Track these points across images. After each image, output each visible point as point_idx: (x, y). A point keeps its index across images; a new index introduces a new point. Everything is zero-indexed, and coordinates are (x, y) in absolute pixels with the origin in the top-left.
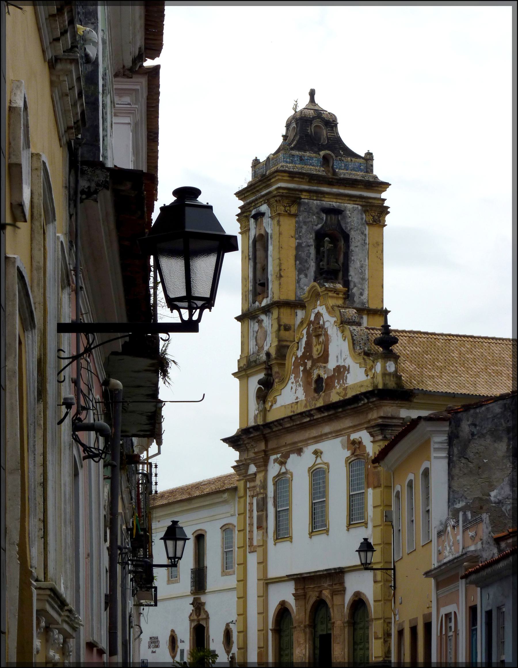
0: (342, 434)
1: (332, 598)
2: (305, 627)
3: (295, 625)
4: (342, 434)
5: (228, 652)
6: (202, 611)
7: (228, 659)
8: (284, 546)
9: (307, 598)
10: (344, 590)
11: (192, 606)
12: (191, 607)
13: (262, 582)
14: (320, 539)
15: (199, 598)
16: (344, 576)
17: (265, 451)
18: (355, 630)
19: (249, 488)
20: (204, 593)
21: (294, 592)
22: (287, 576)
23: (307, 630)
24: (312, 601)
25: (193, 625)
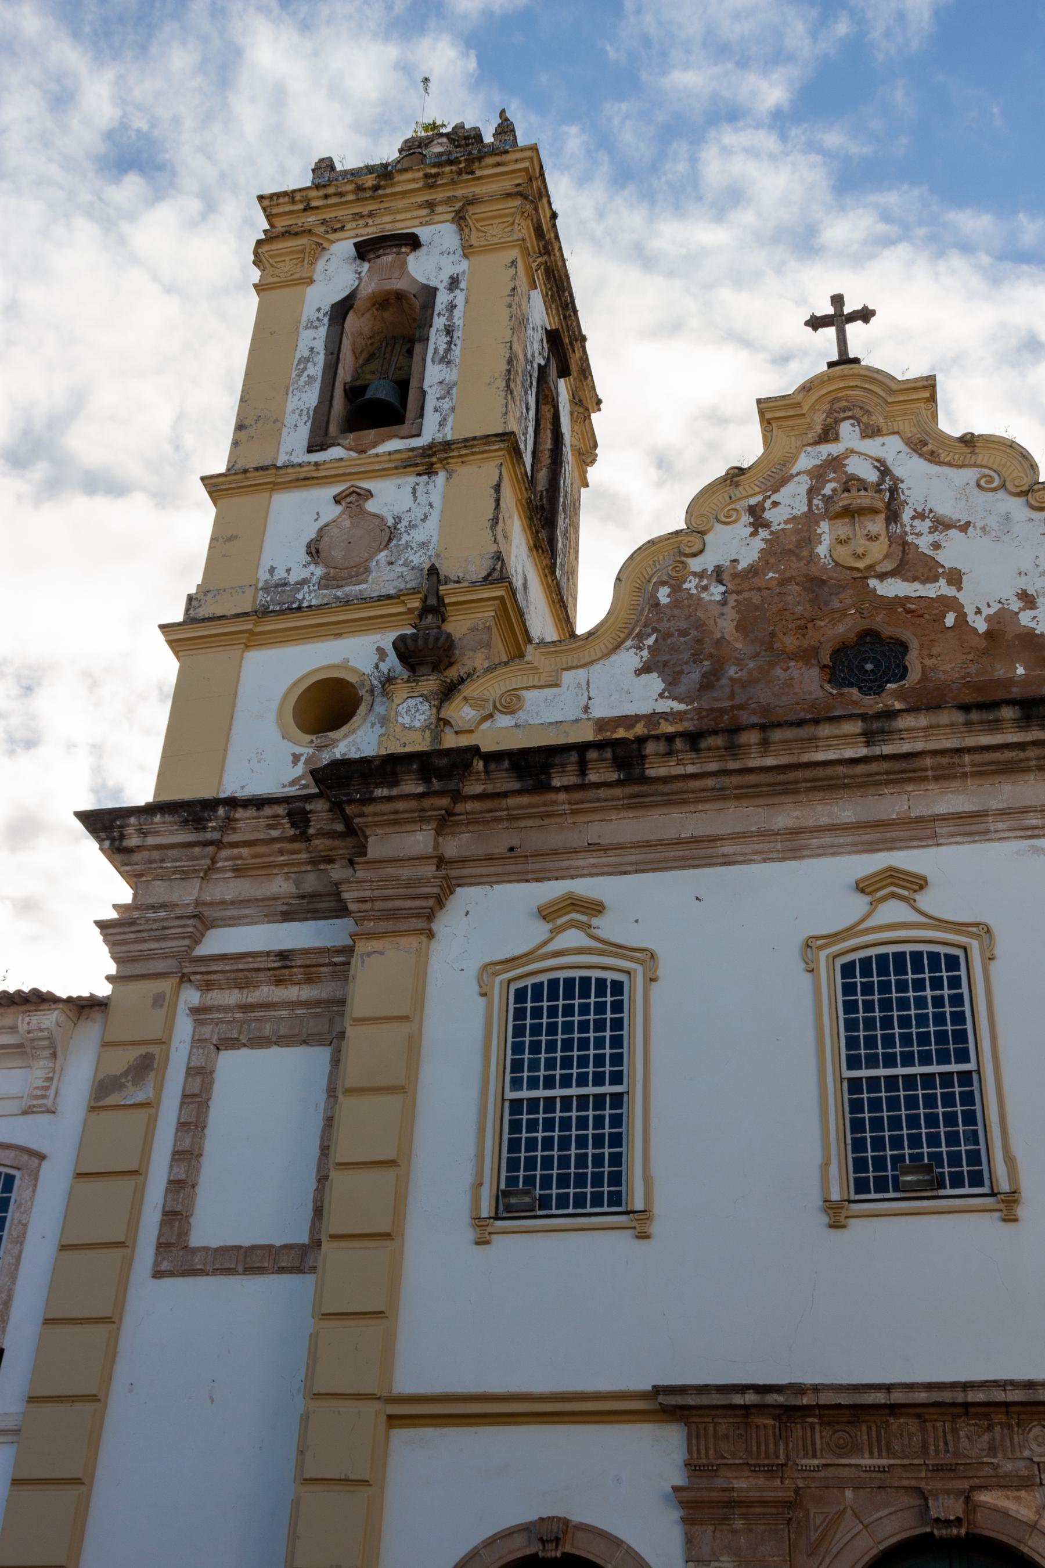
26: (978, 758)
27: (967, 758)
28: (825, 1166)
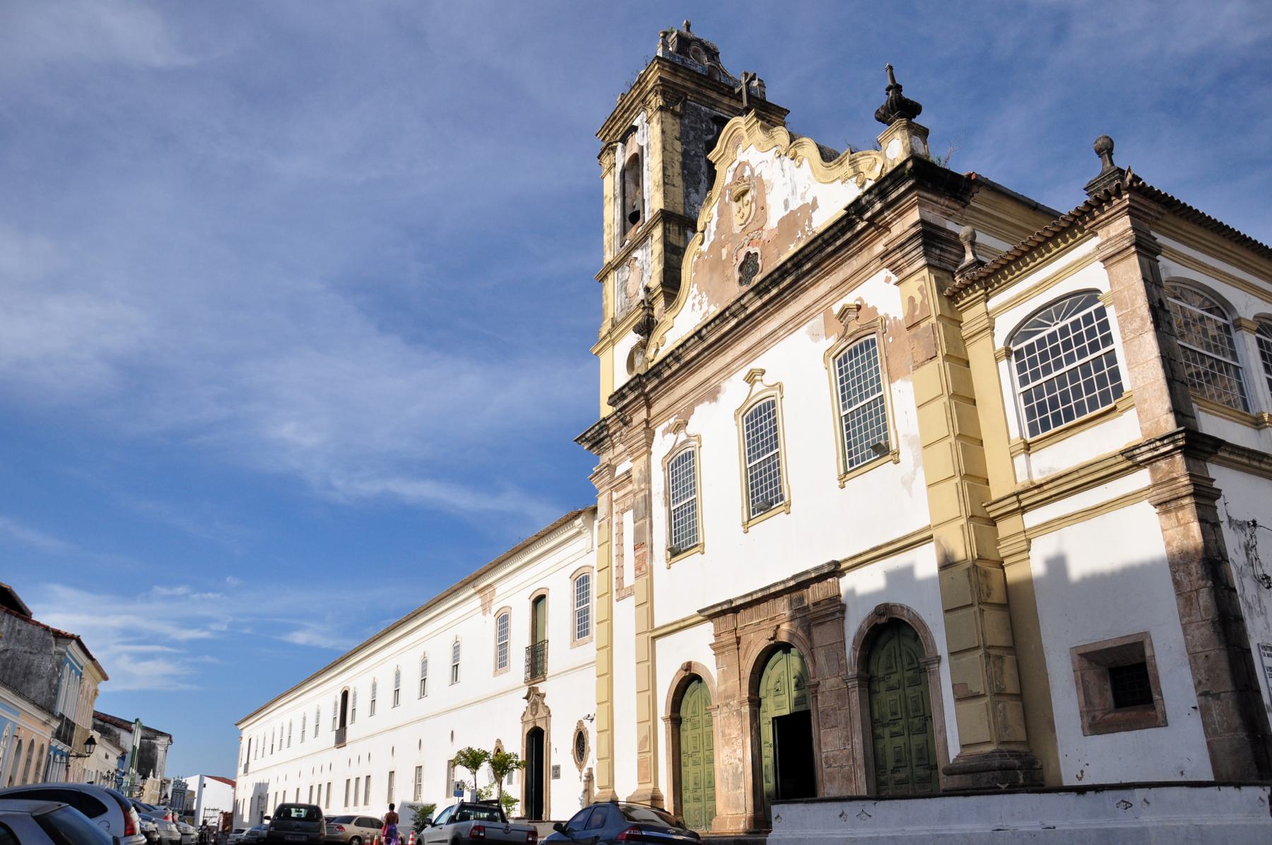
1: (809, 634)
2: (741, 703)
3: (715, 703)
5: (580, 767)
6: (540, 705)
7: (581, 778)
8: (687, 563)
9: (743, 645)
11: (526, 701)
14: (773, 524)
15: (537, 688)
21: (713, 640)
22: (700, 612)
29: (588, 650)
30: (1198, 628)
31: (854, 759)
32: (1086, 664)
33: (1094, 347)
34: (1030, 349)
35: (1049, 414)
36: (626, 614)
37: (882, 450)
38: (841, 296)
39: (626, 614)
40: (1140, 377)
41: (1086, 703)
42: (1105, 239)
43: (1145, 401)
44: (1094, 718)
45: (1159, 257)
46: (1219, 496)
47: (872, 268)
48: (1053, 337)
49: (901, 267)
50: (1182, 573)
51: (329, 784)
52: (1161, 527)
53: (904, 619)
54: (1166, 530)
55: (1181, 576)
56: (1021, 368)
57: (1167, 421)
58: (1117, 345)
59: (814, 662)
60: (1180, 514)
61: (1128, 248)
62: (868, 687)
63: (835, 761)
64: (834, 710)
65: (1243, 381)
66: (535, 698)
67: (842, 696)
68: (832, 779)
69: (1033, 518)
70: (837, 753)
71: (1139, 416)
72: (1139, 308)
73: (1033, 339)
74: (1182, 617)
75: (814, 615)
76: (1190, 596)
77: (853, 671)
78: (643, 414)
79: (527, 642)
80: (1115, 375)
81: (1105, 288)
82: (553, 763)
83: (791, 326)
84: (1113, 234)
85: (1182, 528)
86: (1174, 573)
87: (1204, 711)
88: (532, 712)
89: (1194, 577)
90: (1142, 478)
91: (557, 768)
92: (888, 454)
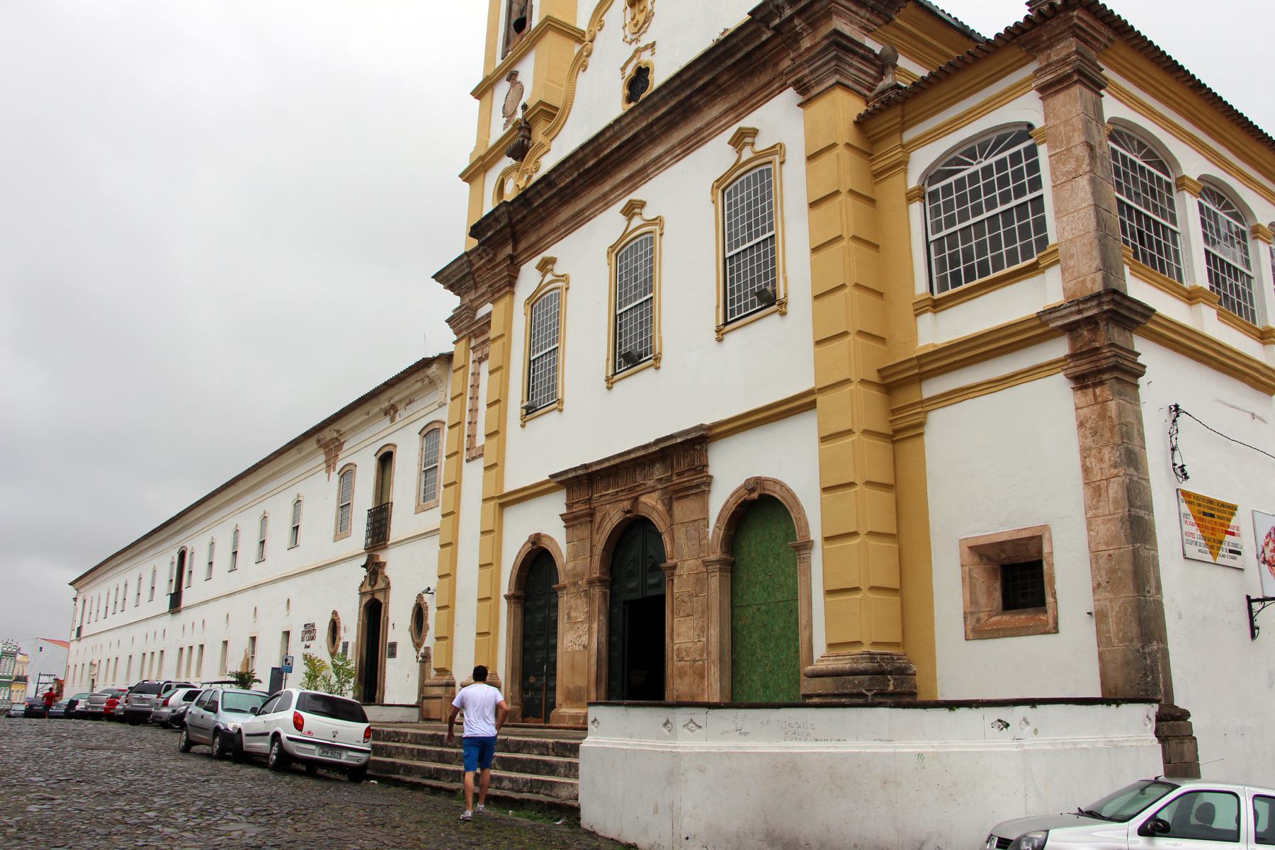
0: (704, 138)
1: (670, 510)
3: (563, 579)
4: (704, 138)
5: (418, 646)
7: (417, 658)
8: (546, 423)
9: (598, 518)
10: (708, 481)
11: (365, 569)
12: (364, 572)
13: (492, 503)
14: (640, 382)
15: (378, 556)
16: (706, 451)
17: (512, 258)
18: (734, 581)
19: (473, 348)
20: (385, 547)
21: (565, 511)
22: (552, 477)
23: (597, 591)
24: (608, 527)
25: (365, 601)
26: (659, 125)
27: (655, 128)
28: (608, 360)
29: (433, 519)
30: (1104, 523)
31: (709, 653)
32: (976, 559)
33: (1020, 192)
34: (947, 190)
35: (962, 267)
36: (473, 475)
37: (769, 300)
38: (738, 118)
39: (473, 475)
40: (1068, 228)
41: (972, 603)
42: (1044, 63)
43: (1072, 256)
44: (978, 620)
45: (1102, 92)
46: (1141, 374)
47: (775, 86)
48: (974, 177)
49: (808, 85)
50: (1093, 459)
51: (162, 652)
52: (1075, 404)
53: (776, 495)
54: (1081, 408)
55: (1092, 462)
56: (936, 211)
57: (1094, 281)
58: (1046, 190)
59: (673, 540)
60: (1098, 391)
61: (1069, 76)
62: (731, 572)
63: (688, 655)
64: (691, 596)
65: (1179, 248)
66: (374, 569)
67: (700, 581)
68: (682, 674)
69: (932, 388)
70: (690, 645)
71: (1063, 273)
72: (1076, 146)
73: (951, 180)
74: (1088, 509)
75: (677, 487)
76: (1099, 486)
77: (716, 554)
78: (508, 250)
79: (370, 504)
80: (1041, 225)
81: (1039, 123)
82: (390, 640)
83: (678, 152)
84: (1054, 58)
85: (1099, 406)
86: (1084, 458)
87: (1099, 616)
88: (370, 581)
89: (1105, 465)
90: (1059, 348)
91: (393, 645)
92: (774, 304)
